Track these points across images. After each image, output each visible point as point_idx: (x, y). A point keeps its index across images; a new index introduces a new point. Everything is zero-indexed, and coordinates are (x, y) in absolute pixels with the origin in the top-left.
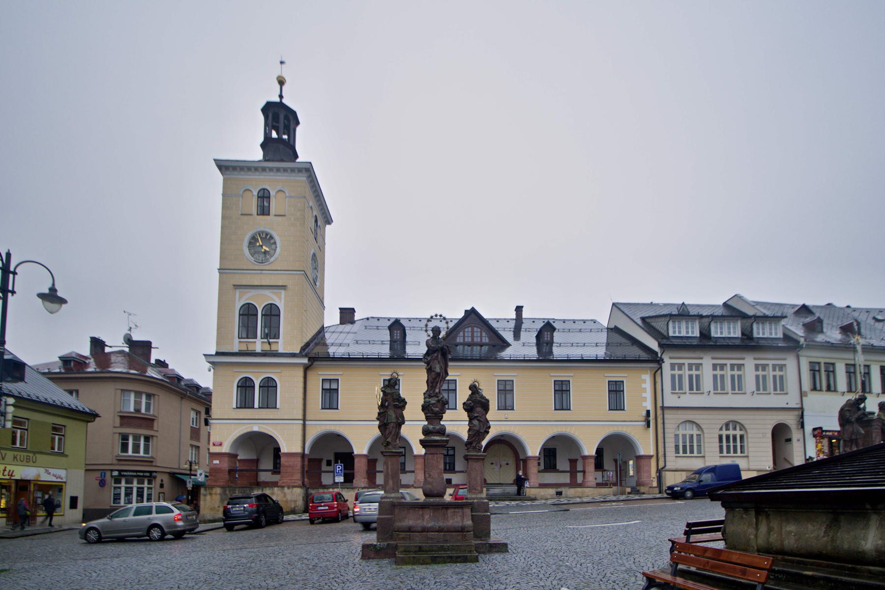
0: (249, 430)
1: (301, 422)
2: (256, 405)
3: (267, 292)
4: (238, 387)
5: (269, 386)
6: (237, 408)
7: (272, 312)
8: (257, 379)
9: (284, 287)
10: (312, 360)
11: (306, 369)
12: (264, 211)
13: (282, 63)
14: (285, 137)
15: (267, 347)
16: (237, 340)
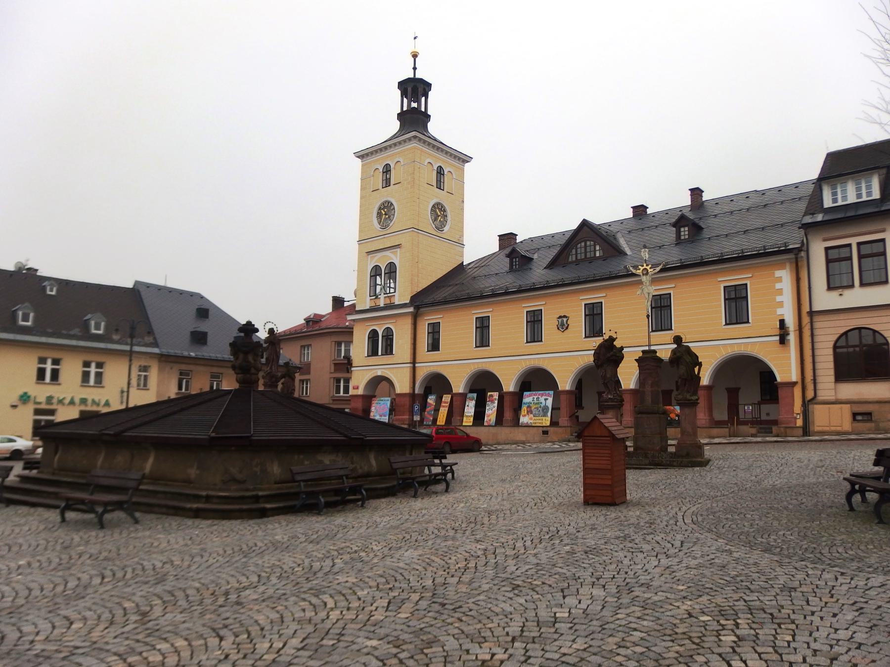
0: (375, 375)
1: (411, 365)
2: (380, 353)
3: (388, 253)
4: (369, 338)
5: (389, 336)
6: (368, 356)
7: (391, 270)
8: (380, 330)
9: (398, 246)
10: (417, 308)
11: (415, 317)
12: (387, 183)
13: (415, 38)
14: (414, 105)
15: (388, 302)
16: (368, 298)
